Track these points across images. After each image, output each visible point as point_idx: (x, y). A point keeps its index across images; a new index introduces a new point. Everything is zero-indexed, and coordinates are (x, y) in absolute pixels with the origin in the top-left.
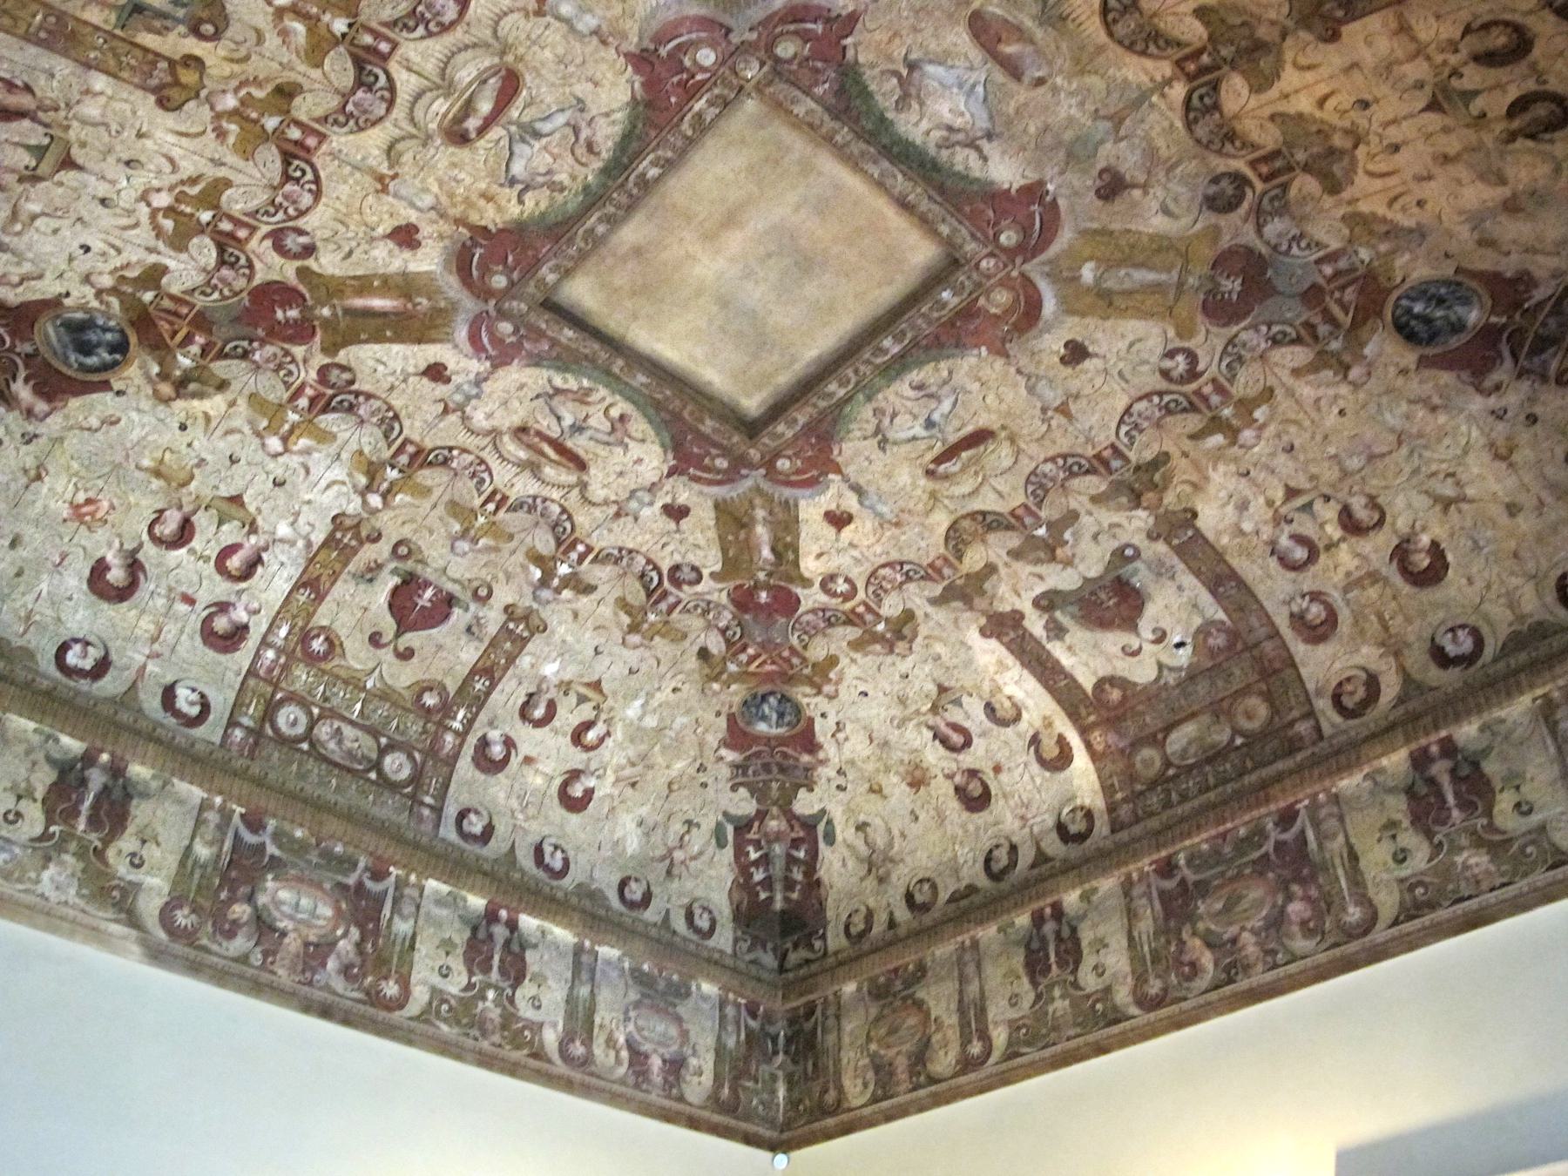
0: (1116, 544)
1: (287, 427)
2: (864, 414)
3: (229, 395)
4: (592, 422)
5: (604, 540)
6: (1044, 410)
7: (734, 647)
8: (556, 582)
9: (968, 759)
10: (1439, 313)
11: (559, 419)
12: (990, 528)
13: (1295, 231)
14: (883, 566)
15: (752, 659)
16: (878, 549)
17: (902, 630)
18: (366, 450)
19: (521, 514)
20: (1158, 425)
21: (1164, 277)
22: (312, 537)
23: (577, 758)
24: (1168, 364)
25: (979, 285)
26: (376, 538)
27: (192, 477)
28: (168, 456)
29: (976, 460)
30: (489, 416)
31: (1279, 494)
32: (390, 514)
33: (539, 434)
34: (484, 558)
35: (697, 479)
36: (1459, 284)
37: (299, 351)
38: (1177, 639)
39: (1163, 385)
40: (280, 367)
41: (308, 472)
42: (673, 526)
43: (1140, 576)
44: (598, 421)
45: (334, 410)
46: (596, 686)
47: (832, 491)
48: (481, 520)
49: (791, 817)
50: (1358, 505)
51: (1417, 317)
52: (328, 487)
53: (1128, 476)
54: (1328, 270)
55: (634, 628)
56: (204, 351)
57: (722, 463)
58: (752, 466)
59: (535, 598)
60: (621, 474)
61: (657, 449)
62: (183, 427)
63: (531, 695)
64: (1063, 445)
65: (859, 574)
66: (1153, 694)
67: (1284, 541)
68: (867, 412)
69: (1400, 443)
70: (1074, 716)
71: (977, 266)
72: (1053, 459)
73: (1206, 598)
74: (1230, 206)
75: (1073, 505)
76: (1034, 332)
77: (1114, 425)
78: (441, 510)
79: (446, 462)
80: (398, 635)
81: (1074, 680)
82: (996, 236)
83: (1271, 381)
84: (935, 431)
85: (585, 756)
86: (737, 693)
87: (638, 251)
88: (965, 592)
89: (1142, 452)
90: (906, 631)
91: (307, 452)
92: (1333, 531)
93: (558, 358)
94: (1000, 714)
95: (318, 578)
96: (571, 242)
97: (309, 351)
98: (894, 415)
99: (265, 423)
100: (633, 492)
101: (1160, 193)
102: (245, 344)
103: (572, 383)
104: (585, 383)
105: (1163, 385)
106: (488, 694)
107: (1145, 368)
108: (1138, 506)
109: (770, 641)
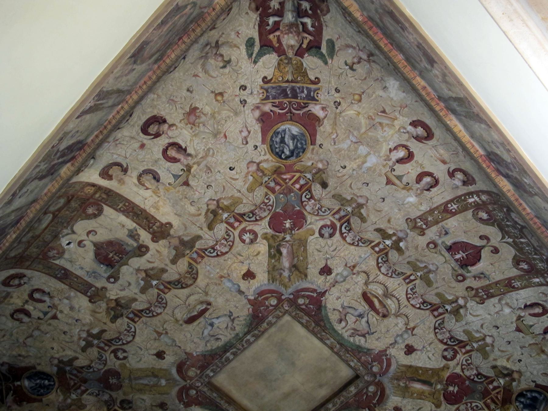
0: (120, 282)
1: (480, 343)
2: (239, 328)
3: (494, 363)
4: (354, 319)
5: (364, 252)
6: (167, 333)
7: (307, 188)
8: (394, 238)
9: (163, 141)
10: (38, 381)
11: (368, 322)
12: (178, 281)
13: (99, 397)
14: (227, 253)
15: (297, 181)
16: (229, 262)
17: (213, 216)
18: (454, 320)
19: (400, 270)
20: (120, 333)
21: (137, 382)
22: (497, 301)
23: (414, 146)
24: (125, 354)
25: (200, 377)
26: (469, 288)
27: (530, 345)
28: (533, 355)
29: (189, 312)
30: (396, 325)
31: (59, 315)
32: (457, 294)
33: (377, 312)
34: (424, 259)
35: (314, 291)
36: (38, 395)
37: (458, 370)
38: (72, 245)
39: (124, 347)
40: (469, 364)
41: (482, 326)
42: (329, 263)
43: (102, 269)
44: (351, 319)
45: (458, 340)
46: (389, 182)
47: (252, 291)
48: (419, 274)
49: (280, 51)
50: (26, 319)
51: (45, 379)
52: (477, 316)
53: (125, 312)
54: (83, 388)
55: (360, 206)
56: (491, 382)
57: (301, 301)
58: (289, 300)
59: (407, 235)
60: (348, 290)
61: (329, 306)
62: (520, 361)
63: (428, 190)
64: (155, 320)
65: (238, 246)
66: (70, 222)
67: (46, 298)
68: (238, 329)
69: (24, 343)
70: (108, 192)
71: (202, 384)
72: (158, 314)
73: (68, 266)
74: (122, 402)
75: (144, 296)
76: (177, 363)
77: (137, 331)
78: (435, 285)
79: (424, 302)
80: (483, 247)
81: (114, 209)
82: (197, 393)
83: (84, 354)
84: (209, 322)
85: (409, 144)
86: (309, 159)
87: (321, 386)
88: (185, 246)
89: (122, 323)
90: (211, 216)
91: (477, 331)
92: (29, 307)
93: (359, 352)
94: (150, 177)
95: (506, 286)
96: (342, 402)
97: (454, 368)
98: (227, 328)
99: (487, 348)
100: (344, 280)
101: (146, 404)
102: (476, 379)
103: (357, 338)
104: (352, 339)
105: (124, 347)
106: (452, 201)
107: (133, 352)
108: (116, 300)
109: (286, 195)
